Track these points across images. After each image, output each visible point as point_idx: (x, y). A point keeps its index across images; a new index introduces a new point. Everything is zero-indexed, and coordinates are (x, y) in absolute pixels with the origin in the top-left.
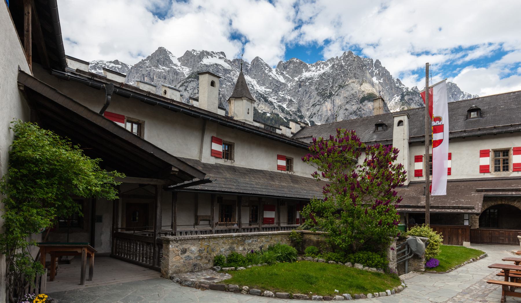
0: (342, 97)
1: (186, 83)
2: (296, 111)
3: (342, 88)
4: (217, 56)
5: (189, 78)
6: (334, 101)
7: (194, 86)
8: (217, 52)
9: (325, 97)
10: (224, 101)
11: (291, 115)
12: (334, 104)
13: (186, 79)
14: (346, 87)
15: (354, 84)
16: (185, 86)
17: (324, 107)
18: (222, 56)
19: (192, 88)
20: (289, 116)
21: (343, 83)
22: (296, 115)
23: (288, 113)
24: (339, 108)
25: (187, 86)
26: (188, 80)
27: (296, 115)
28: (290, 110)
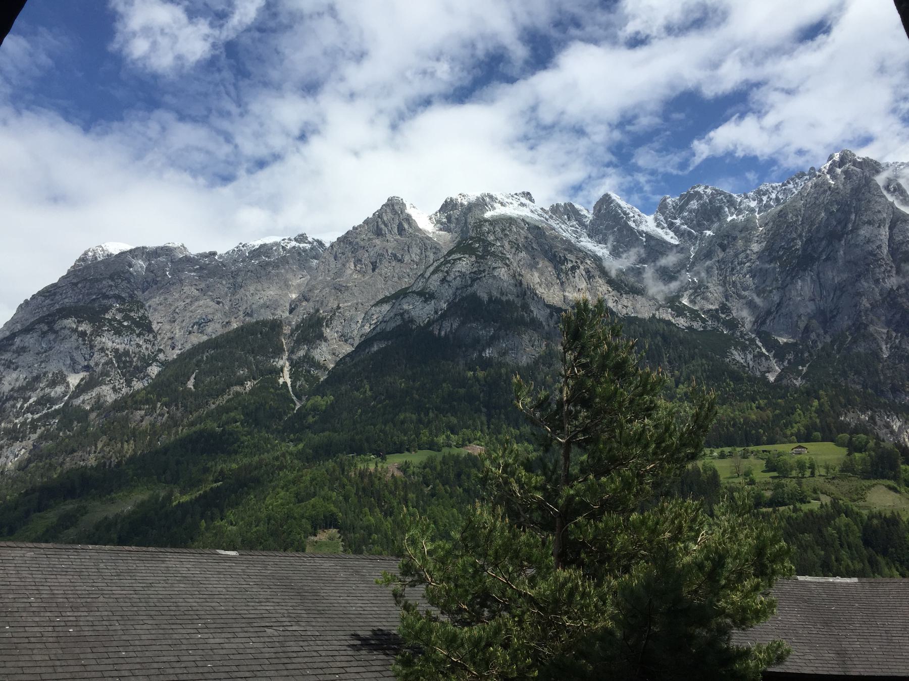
0: (840, 262)
1: (445, 264)
2: (717, 310)
3: (840, 241)
4: (514, 202)
5: (451, 253)
6: (821, 275)
7: (464, 270)
8: (513, 193)
9: (793, 269)
10: (533, 299)
11: (703, 320)
12: (820, 284)
13: (444, 256)
14: (850, 236)
15: (871, 227)
16: (442, 271)
17: (794, 293)
18: (524, 200)
19: (457, 274)
20: (700, 323)
21: (839, 228)
22: (718, 319)
23: (695, 315)
24: (838, 293)
25: (447, 272)
26: (449, 259)
27: (718, 319)
28: (702, 309)
